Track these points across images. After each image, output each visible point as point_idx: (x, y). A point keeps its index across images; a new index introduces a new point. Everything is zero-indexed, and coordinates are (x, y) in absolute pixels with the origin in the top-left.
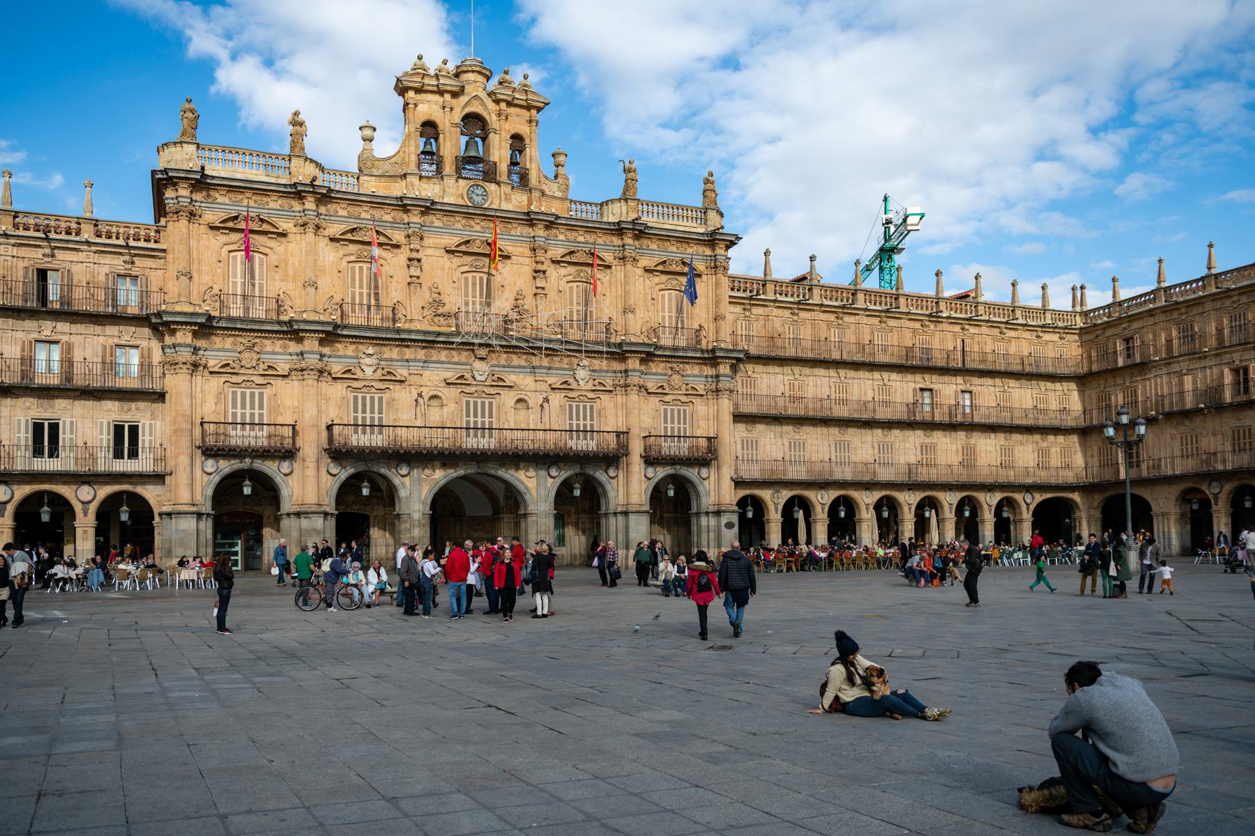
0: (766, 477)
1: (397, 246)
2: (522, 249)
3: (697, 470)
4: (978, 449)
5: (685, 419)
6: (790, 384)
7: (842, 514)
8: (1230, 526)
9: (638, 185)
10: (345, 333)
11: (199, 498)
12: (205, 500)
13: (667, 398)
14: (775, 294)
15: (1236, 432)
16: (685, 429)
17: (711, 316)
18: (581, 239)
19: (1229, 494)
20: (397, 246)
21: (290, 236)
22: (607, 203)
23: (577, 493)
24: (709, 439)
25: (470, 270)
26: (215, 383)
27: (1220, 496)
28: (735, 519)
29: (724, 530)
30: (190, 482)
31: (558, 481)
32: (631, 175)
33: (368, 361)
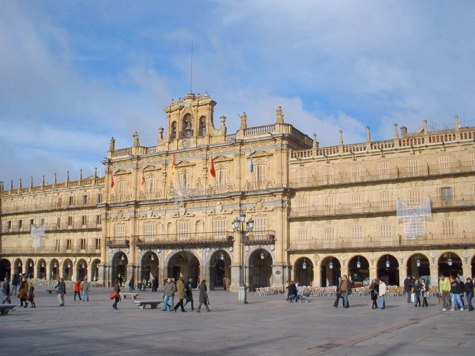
0: (339, 246)
1: (161, 169)
2: (200, 161)
4: (455, 223)
6: (326, 199)
7: (388, 265)
10: (141, 203)
11: (108, 261)
12: (110, 262)
13: (256, 214)
18: (221, 151)
20: (161, 169)
21: (132, 173)
25: (182, 173)
26: (112, 224)
30: (104, 256)
31: (211, 254)
33: (149, 212)
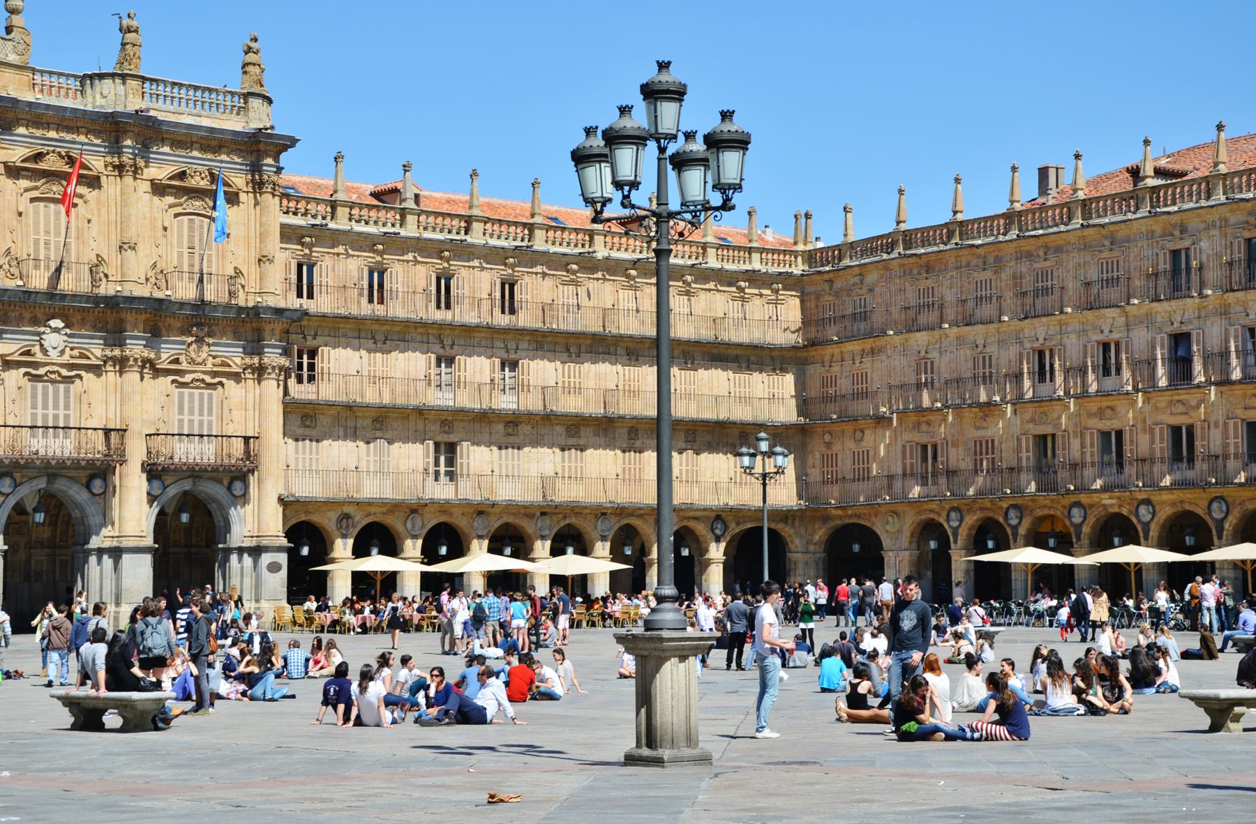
3: (226, 483)
5: (210, 409)
8: (972, 573)
9: (142, 52)
14: (350, 220)
15: (978, 444)
16: (210, 423)
17: (254, 256)
19: (970, 529)
22: (92, 77)
23: (40, 517)
24: (247, 439)
27: (960, 530)
28: (283, 558)
29: (265, 573)
32: (130, 37)
